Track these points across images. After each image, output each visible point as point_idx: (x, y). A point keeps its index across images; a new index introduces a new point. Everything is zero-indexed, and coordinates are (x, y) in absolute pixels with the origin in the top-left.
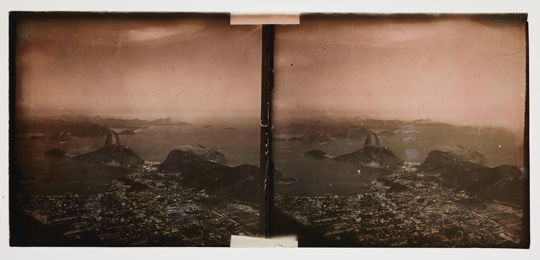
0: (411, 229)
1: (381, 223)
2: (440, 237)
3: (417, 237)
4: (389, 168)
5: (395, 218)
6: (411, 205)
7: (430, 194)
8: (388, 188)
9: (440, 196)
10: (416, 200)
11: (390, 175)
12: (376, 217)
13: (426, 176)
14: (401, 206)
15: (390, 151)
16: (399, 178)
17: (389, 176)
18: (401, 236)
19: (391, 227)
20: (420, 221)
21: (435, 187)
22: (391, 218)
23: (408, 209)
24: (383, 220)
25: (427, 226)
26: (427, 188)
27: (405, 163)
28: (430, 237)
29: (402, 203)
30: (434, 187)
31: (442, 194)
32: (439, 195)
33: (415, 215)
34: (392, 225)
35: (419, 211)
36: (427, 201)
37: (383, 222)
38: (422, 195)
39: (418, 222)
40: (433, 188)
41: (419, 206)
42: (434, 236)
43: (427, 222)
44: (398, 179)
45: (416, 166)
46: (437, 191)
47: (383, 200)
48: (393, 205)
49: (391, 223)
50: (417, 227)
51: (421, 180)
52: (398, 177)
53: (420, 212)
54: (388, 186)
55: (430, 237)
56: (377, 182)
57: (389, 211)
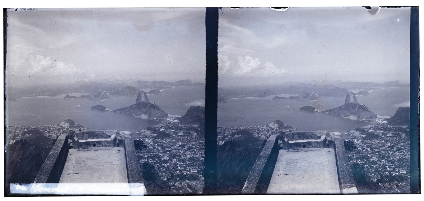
0: (174, 168)
1: (150, 162)
2: (198, 176)
3: (179, 175)
4: (156, 119)
5: (161, 159)
6: (174, 149)
7: (190, 141)
8: (155, 135)
9: (198, 143)
10: (178, 146)
11: (157, 125)
12: (145, 157)
13: (187, 126)
14: (166, 150)
15: (157, 106)
16: (163, 127)
17: (156, 126)
18: (166, 173)
19: (158, 166)
20: (181, 162)
21: (194, 136)
22: (158, 159)
23: (172, 152)
24: (151, 160)
25: (187, 167)
26: (187, 136)
27: (169, 116)
28: (189, 175)
29: (166, 147)
30: (194, 135)
31: (200, 142)
32: (198, 142)
33: (177, 158)
34: (159, 165)
35: (181, 154)
36: (187, 146)
37: (151, 162)
38: (183, 142)
39: (179, 163)
40: (192, 136)
41: (181, 150)
42: (193, 175)
43: (188, 164)
44: (163, 128)
45: (178, 119)
46: (196, 139)
47: (151, 145)
48: (159, 149)
49: (157, 163)
50: (179, 167)
51: (182, 130)
52: (163, 127)
53: (182, 155)
54: (155, 134)
55: (189, 175)
56: (146, 130)
57: (156, 153)
